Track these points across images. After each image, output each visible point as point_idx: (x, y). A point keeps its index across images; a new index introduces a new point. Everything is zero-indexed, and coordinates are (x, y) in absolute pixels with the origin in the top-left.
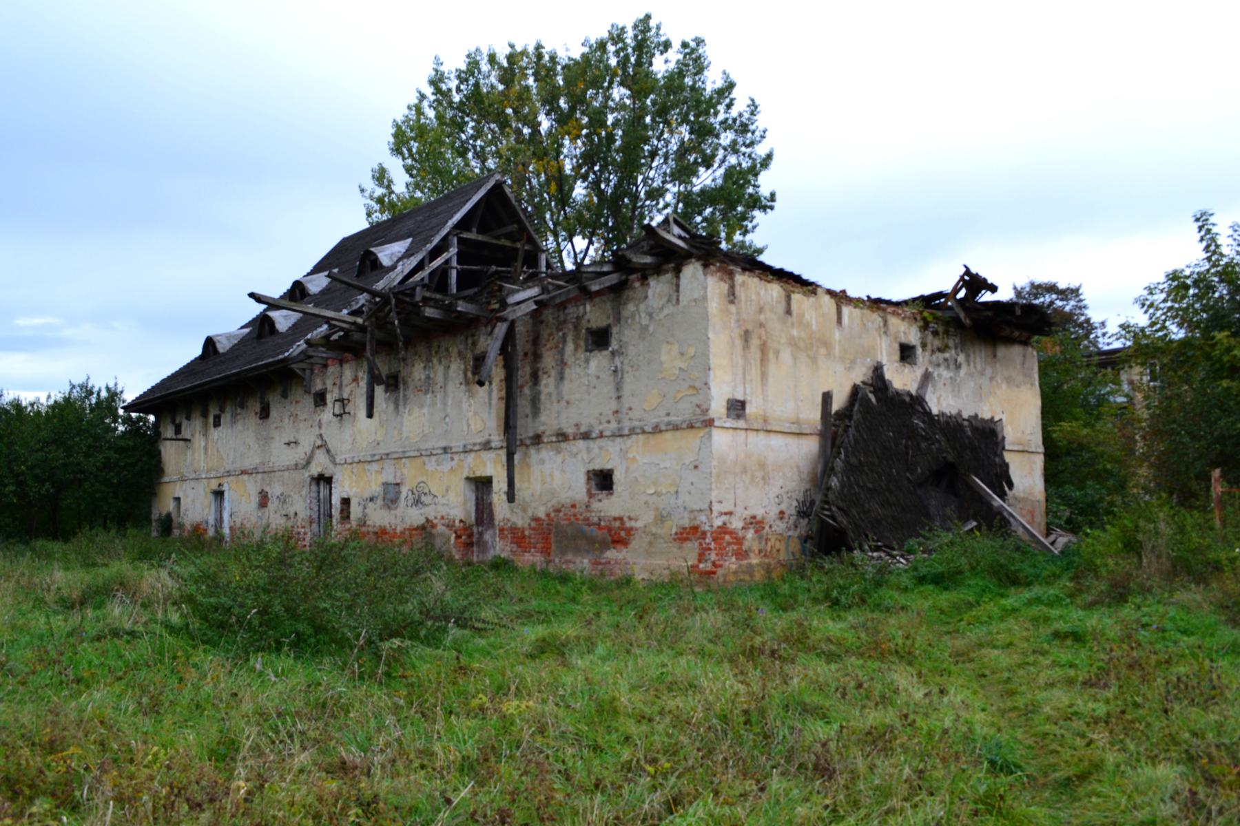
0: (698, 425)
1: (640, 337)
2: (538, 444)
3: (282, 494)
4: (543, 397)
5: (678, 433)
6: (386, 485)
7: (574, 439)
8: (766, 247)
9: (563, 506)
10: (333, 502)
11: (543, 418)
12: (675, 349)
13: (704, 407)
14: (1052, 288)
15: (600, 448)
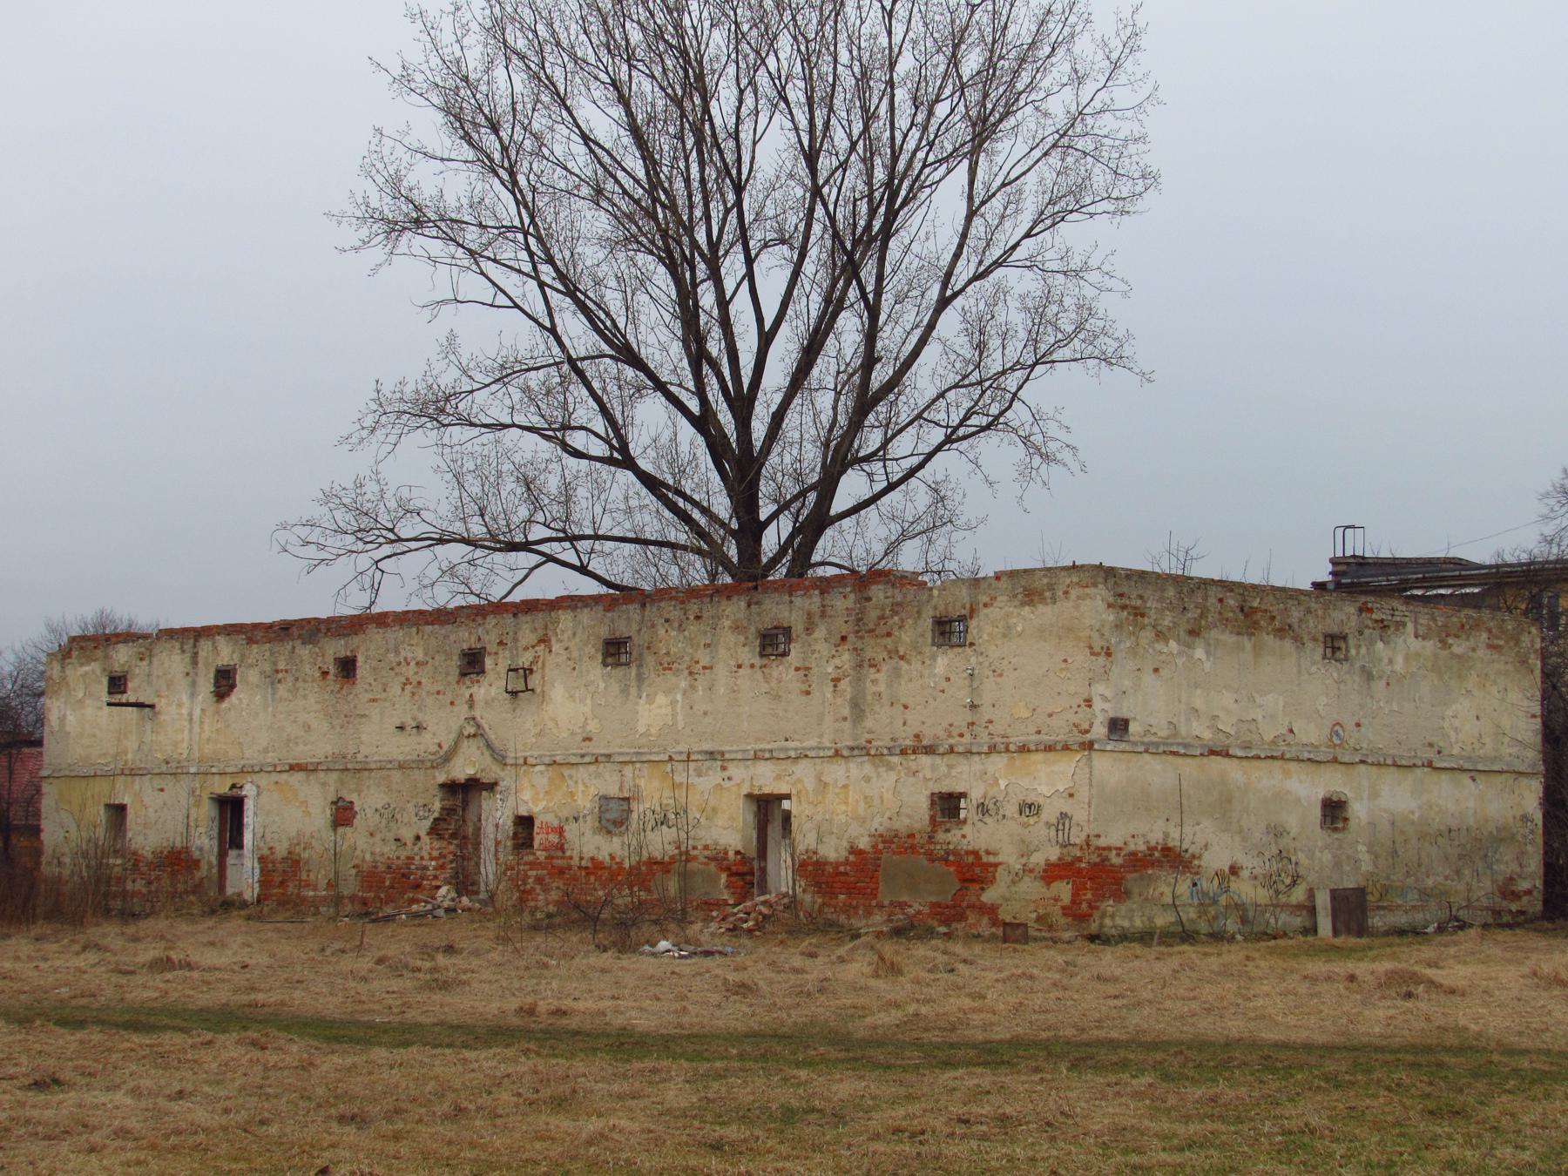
5: (1051, 755)
7: (914, 752)
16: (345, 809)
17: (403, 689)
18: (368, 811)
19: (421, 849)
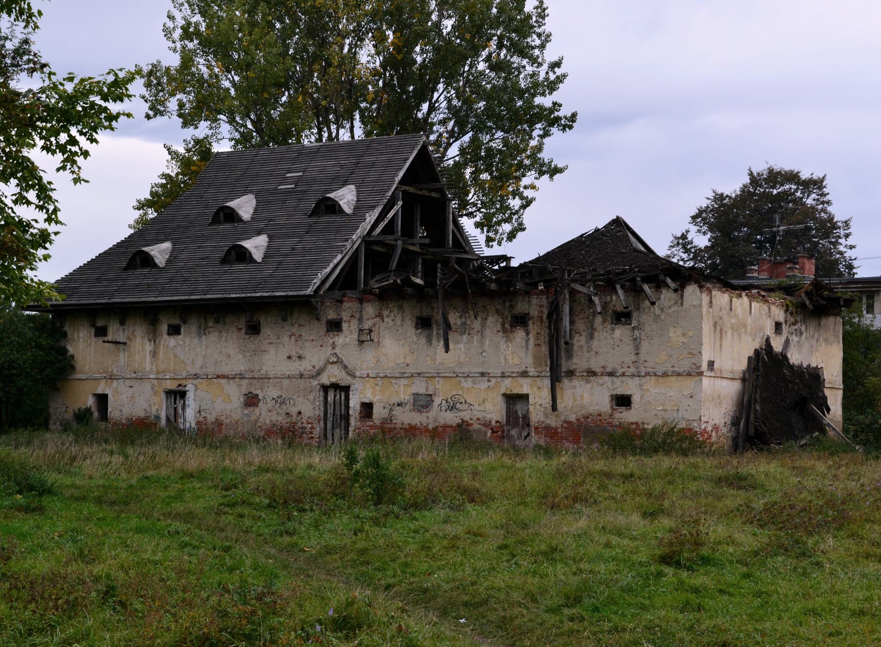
0: (694, 374)
1: (654, 321)
2: (571, 376)
3: (280, 397)
4: (575, 348)
5: (680, 378)
6: (416, 395)
7: (602, 375)
8: (566, 168)
9: (591, 415)
10: (352, 404)
11: (575, 360)
12: (679, 331)
13: (698, 365)
14: (792, 177)
15: (623, 382)
16: (253, 398)
18: (267, 399)
19: (302, 418)
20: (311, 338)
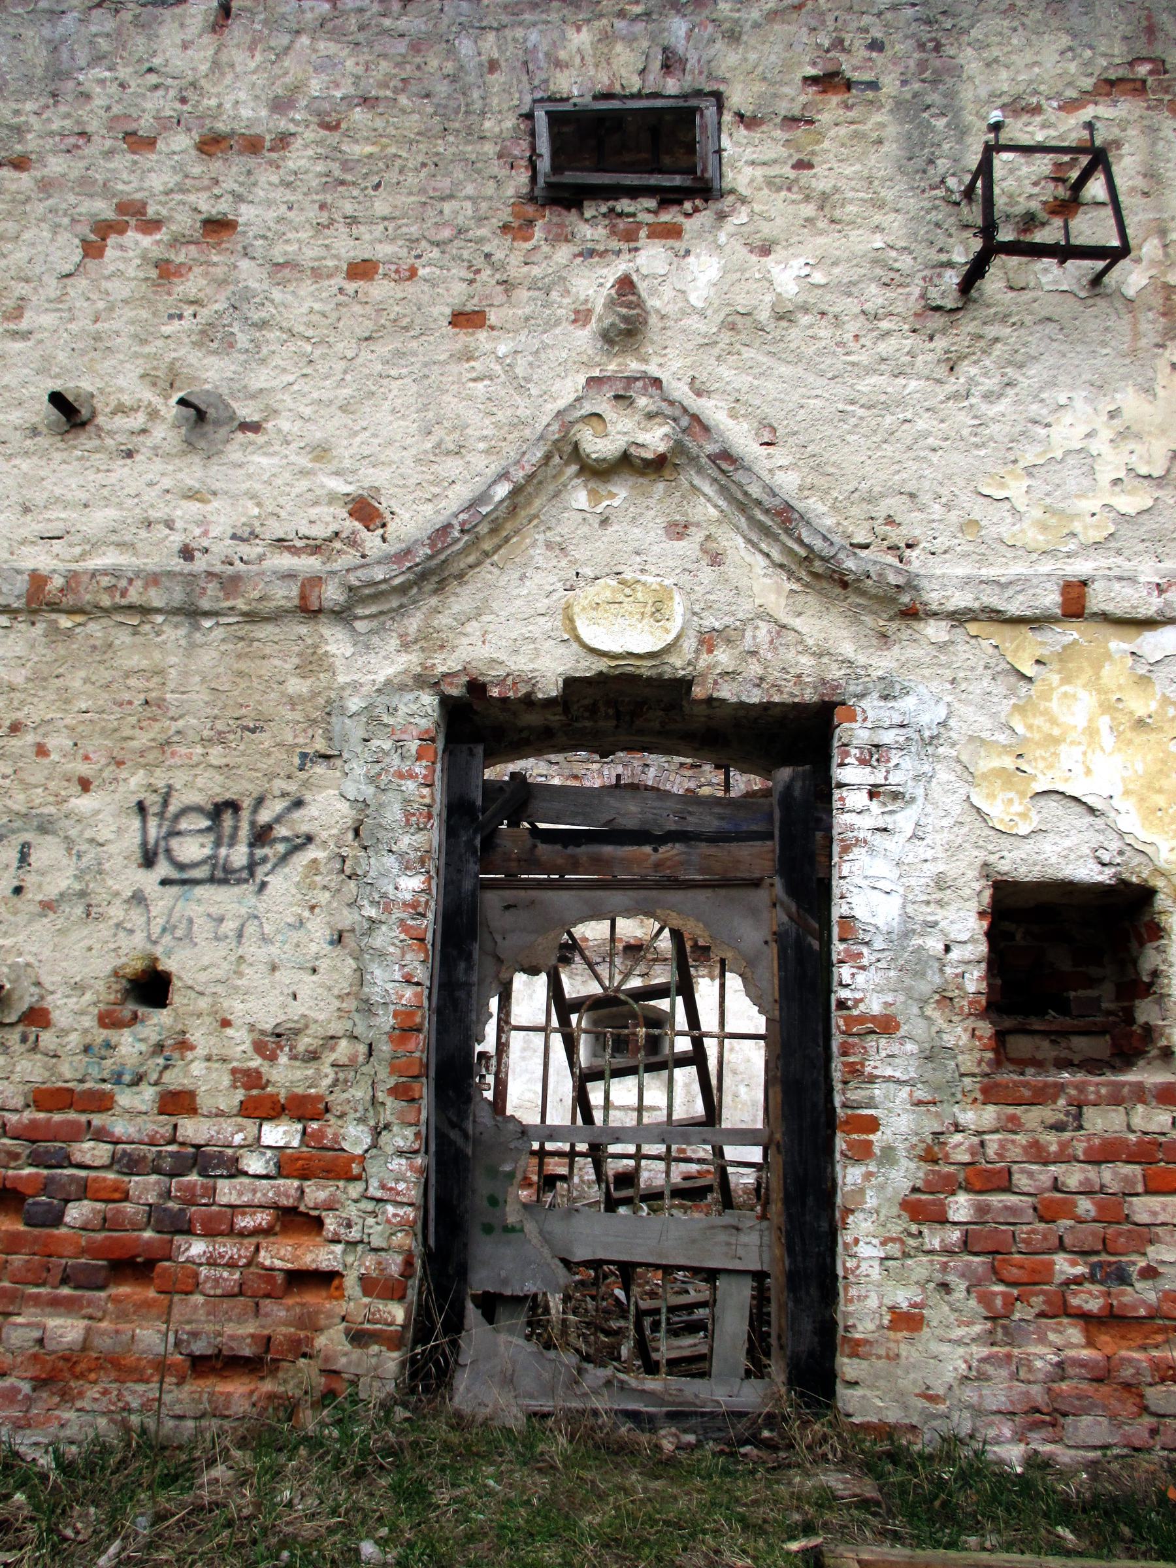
17: (92, 250)
20: (346, 248)
